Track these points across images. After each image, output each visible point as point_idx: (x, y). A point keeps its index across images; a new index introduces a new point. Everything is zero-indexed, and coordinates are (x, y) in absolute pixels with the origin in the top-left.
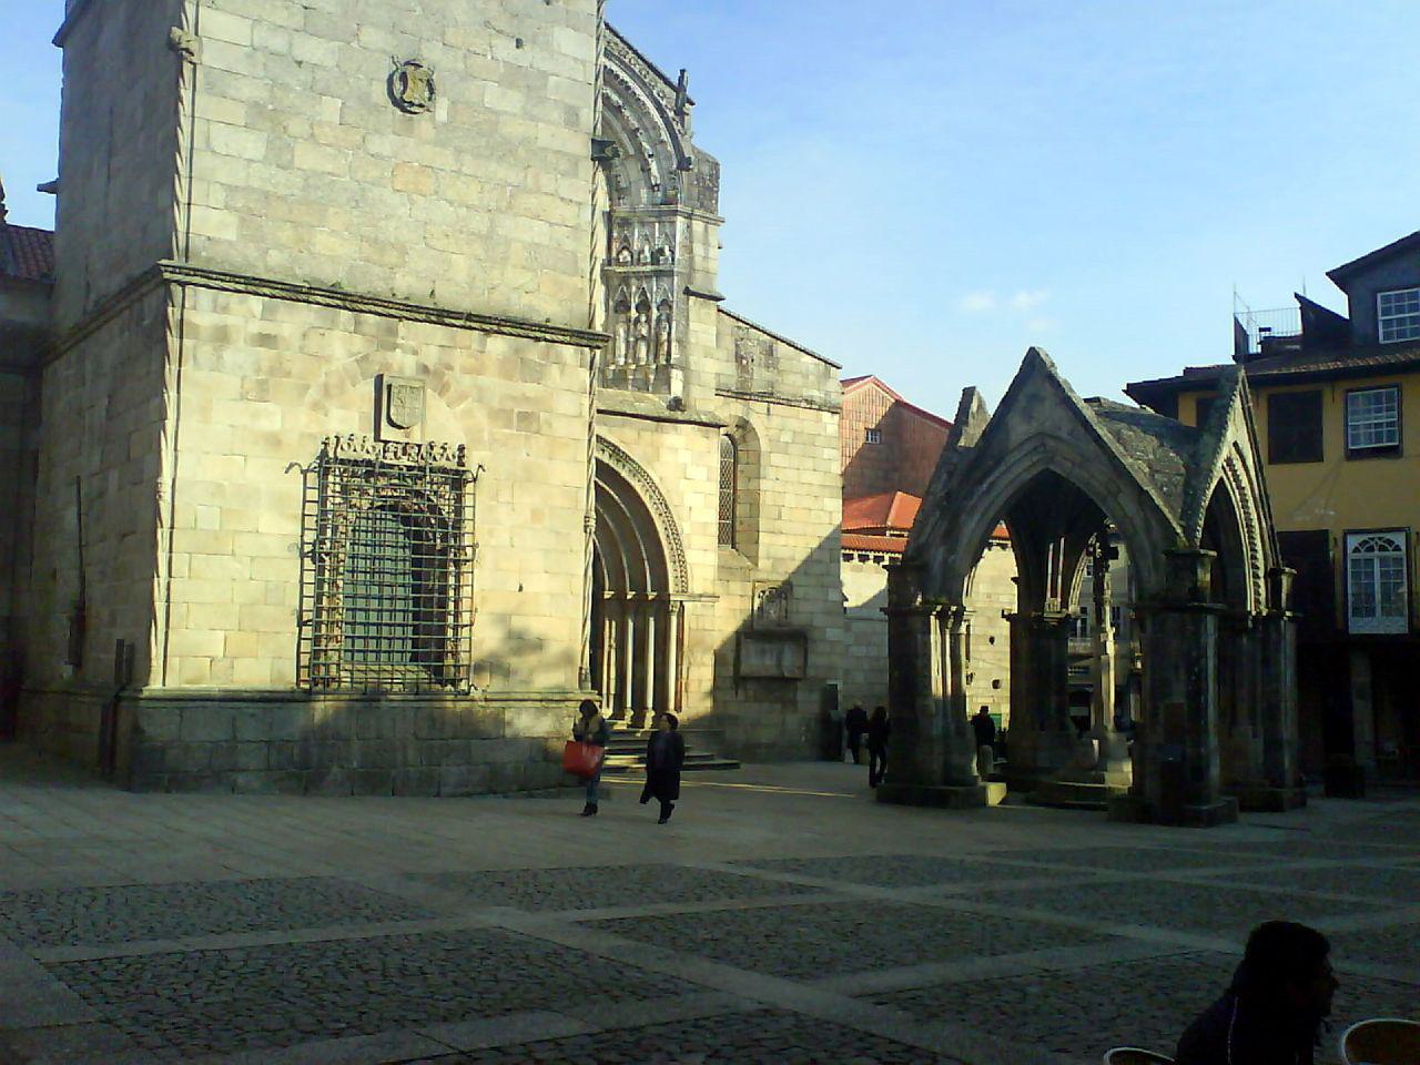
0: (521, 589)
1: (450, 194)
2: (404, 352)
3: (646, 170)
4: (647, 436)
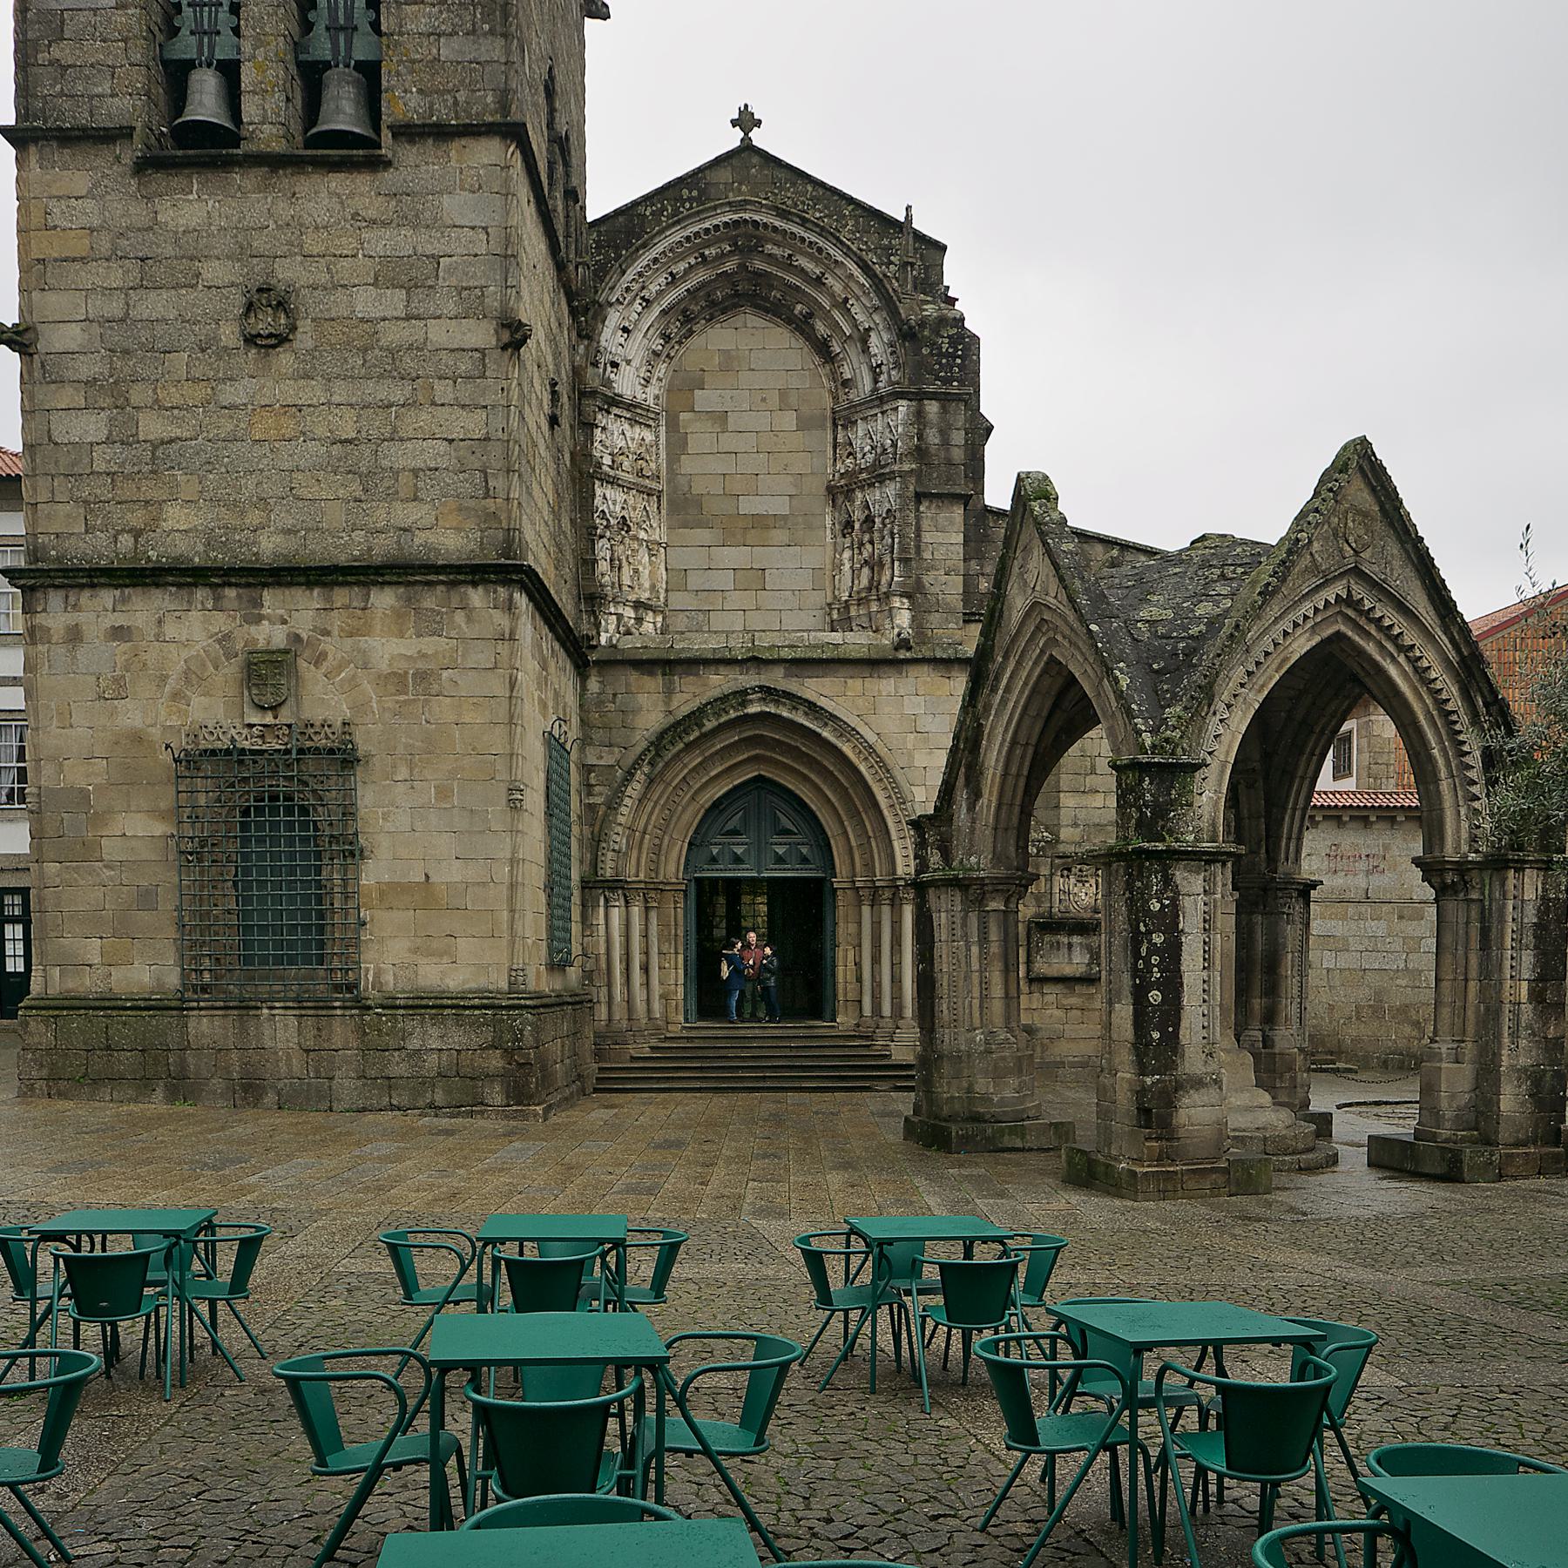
0: (427, 876)
1: (321, 431)
2: (272, 623)
3: (865, 349)
4: (855, 685)
